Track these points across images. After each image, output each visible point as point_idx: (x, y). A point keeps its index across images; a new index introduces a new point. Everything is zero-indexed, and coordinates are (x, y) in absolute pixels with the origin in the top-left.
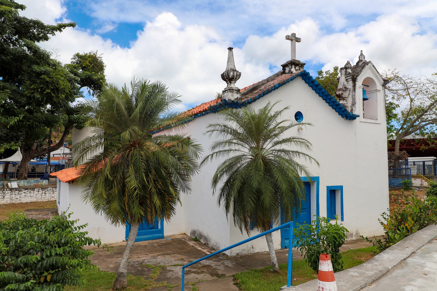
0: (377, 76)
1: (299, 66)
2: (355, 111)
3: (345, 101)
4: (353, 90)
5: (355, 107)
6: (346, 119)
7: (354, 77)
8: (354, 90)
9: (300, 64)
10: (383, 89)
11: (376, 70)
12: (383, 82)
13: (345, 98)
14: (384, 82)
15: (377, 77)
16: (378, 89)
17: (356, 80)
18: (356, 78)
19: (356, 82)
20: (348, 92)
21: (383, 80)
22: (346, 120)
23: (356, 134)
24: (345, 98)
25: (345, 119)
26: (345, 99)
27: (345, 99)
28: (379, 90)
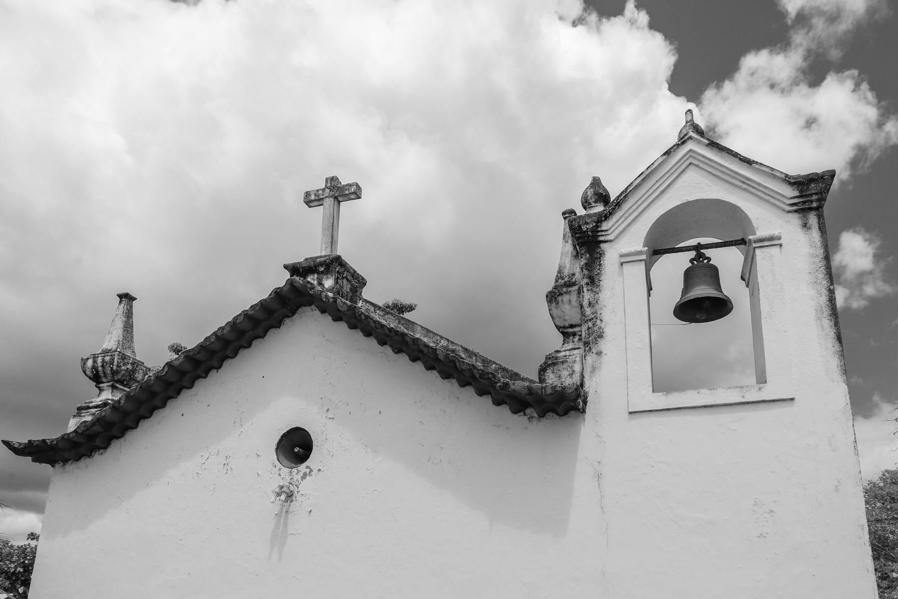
0: (746, 180)
1: (319, 273)
2: (594, 369)
3: (577, 338)
4: (586, 281)
5: (599, 353)
6: (536, 415)
7: (584, 228)
8: (593, 281)
9: (321, 264)
10: (805, 225)
11: (735, 155)
12: (790, 192)
13: (570, 330)
14: (801, 191)
15: (745, 185)
16: (761, 233)
17: (602, 238)
18: (596, 230)
19: (603, 246)
20: (574, 297)
21: (790, 183)
22: (535, 421)
23: (599, 476)
24: (572, 326)
25: (530, 418)
26: (574, 334)
27: (574, 334)
28: (771, 239)
